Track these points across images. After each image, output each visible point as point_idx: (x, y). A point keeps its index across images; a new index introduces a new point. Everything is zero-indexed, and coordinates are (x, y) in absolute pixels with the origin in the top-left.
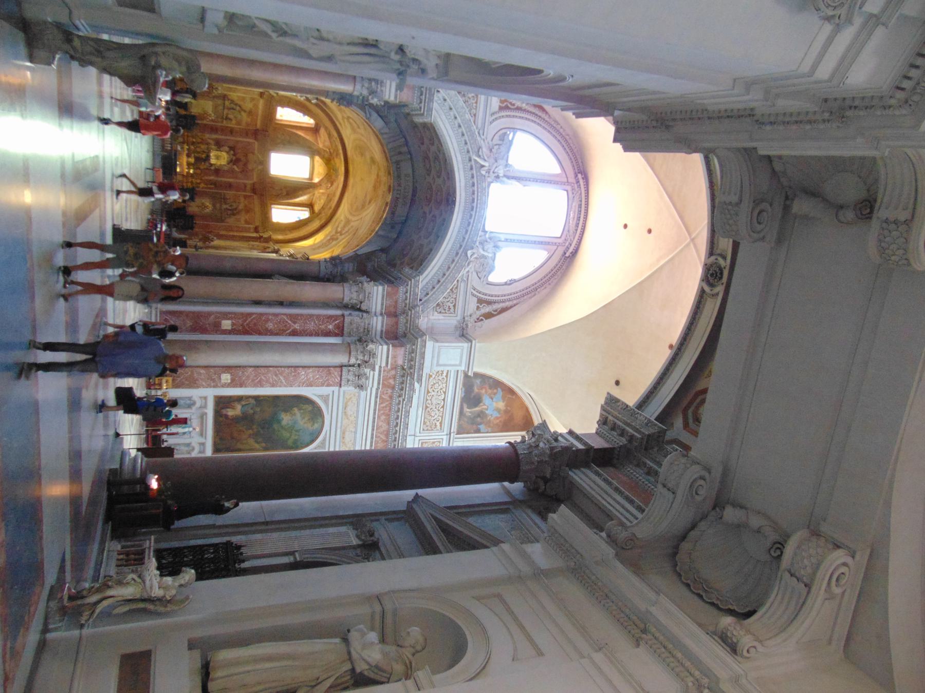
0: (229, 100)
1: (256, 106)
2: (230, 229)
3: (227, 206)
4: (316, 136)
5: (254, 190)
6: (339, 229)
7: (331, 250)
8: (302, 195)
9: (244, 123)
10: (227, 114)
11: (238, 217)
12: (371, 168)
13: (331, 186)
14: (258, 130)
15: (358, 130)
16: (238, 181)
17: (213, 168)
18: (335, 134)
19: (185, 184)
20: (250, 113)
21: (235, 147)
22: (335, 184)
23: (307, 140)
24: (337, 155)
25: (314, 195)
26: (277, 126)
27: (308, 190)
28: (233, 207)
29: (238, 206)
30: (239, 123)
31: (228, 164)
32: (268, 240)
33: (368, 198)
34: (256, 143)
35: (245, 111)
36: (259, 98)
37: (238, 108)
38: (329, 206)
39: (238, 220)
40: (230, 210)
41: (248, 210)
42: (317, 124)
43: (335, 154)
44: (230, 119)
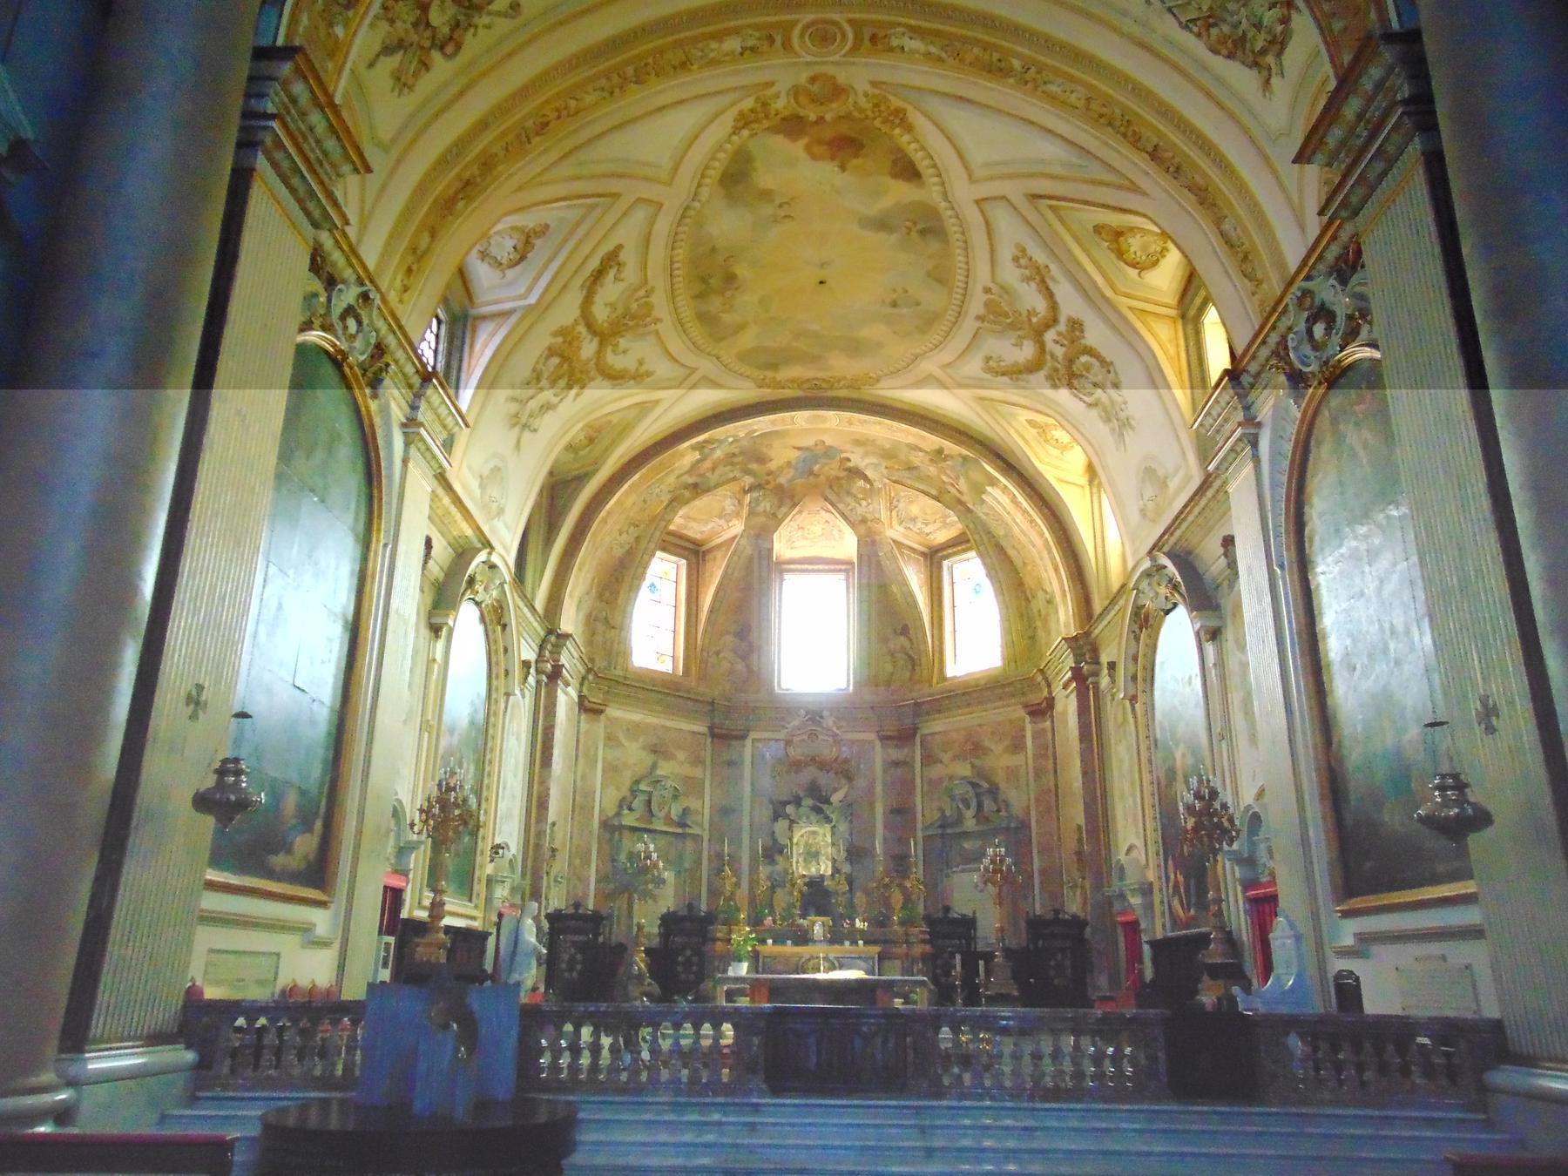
0: (618, 814)
1: (634, 730)
2: (1051, 800)
3: (969, 813)
4: (709, 551)
5: (905, 736)
6: (1027, 351)
7: (1138, 325)
8: (905, 583)
9: (697, 772)
10: (668, 820)
12: (766, 195)
13: (866, 478)
14: (711, 728)
15: (629, 257)
16: (879, 788)
18: (686, 454)
19: (918, 950)
20: (658, 750)
21: (771, 802)
22: (857, 459)
23: (724, 577)
24: (753, 455)
26: (694, 669)
27: (886, 563)
28: (971, 793)
29: (965, 778)
30: (694, 786)
31: (828, 820)
32: (1084, 646)
33: (900, 192)
34: (753, 735)
35: (654, 767)
36: (603, 717)
37: (643, 787)
38: (932, 470)
39: (1012, 773)
40: (980, 806)
41: (975, 748)
43: (754, 466)
44: (686, 811)
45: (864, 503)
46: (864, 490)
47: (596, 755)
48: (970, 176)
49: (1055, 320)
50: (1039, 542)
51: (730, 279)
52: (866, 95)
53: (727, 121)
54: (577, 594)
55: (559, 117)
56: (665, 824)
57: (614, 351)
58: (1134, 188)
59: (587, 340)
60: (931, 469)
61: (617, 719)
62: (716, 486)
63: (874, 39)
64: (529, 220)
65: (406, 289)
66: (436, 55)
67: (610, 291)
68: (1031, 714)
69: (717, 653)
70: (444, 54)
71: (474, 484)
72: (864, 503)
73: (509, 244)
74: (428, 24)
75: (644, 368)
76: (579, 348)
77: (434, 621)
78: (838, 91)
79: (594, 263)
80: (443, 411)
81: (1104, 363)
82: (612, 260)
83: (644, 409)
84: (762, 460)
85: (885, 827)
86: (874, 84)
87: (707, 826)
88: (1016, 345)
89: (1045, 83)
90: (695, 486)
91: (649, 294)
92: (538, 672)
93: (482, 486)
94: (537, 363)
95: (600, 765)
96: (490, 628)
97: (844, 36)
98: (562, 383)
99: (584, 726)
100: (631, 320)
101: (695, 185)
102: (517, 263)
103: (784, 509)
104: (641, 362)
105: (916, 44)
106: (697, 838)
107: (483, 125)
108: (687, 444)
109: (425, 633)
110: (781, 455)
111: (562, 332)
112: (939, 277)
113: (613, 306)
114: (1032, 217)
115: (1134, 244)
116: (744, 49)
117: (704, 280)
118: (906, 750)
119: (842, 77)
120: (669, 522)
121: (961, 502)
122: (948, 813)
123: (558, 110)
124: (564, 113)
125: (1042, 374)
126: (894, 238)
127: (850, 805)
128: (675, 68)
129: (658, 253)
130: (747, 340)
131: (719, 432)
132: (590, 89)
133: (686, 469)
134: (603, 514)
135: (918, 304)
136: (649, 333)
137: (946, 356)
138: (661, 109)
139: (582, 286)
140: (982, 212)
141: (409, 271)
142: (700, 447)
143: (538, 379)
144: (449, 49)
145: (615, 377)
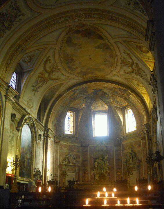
1: (65, 146)
3: (131, 160)
6: (130, 69)
9: (78, 154)
10: (73, 163)
11: (137, 152)
12: (76, 44)
13: (107, 94)
17: (109, 171)
22: (105, 91)
25: (115, 106)
28: (131, 156)
30: (78, 157)
33: (100, 42)
34: (90, 146)
35: (69, 153)
38: (120, 92)
40: (133, 157)
41: (133, 147)
42: (71, 109)
43: (85, 94)
45: (108, 99)
46: (107, 97)
47: (58, 151)
48: (112, 38)
49: (134, 63)
50: (140, 105)
51: (72, 60)
52: (90, 25)
53: (64, 33)
54: (52, 121)
55: (32, 36)
56: (72, 164)
57: (52, 75)
58: (140, 39)
59: (46, 74)
60: (119, 92)
61: (62, 144)
62: (78, 98)
63: (89, 16)
64: (30, 54)
65: (6, 70)
66: (7, 30)
67: (49, 65)
68: (142, 139)
69: (82, 130)
70: (8, 30)
71: (26, 103)
72: (108, 99)
73: (28, 59)
74: (4, 26)
75: (59, 77)
76: (45, 75)
77: (18, 128)
78: (84, 25)
79: (45, 60)
80: (13, 92)
81: (144, 71)
82: (48, 59)
83: (61, 85)
84: (87, 92)
85: (116, 163)
86: (91, 23)
87: (81, 163)
88: (128, 68)
89: (120, 21)
90: (74, 98)
91: (57, 64)
92: (44, 136)
93: (28, 103)
94: (36, 79)
95: (59, 153)
96: (31, 129)
97: (83, 16)
98: (42, 82)
99: (55, 146)
100: (54, 69)
101: (61, 44)
102: (30, 62)
103: (92, 101)
104: (58, 77)
105: (96, 16)
106: (79, 166)
107: (18, 40)
108: (70, 91)
109: (15, 130)
110: (90, 91)
111: (40, 73)
112: (112, 56)
113: (50, 67)
114: (124, 44)
115: (144, 49)
116: (65, 20)
117: (67, 60)
118: (119, 148)
119: (84, 23)
120: (70, 105)
121: (126, 98)
122: (127, 159)
123: (32, 35)
124: (33, 35)
125: (134, 73)
126: (102, 50)
127: (109, 159)
128: (53, 25)
129: (57, 57)
130: (79, 70)
131: (77, 88)
132: (37, 30)
133: (72, 95)
134: (55, 105)
135: (109, 61)
136: (59, 71)
137: (117, 71)
138: (51, 32)
139: (43, 64)
140: (116, 45)
141: (7, 67)
142: (73, 91)
143: (37, 82)
144: (9, 29)
145: (53, 80)
